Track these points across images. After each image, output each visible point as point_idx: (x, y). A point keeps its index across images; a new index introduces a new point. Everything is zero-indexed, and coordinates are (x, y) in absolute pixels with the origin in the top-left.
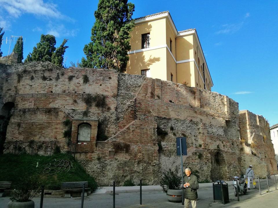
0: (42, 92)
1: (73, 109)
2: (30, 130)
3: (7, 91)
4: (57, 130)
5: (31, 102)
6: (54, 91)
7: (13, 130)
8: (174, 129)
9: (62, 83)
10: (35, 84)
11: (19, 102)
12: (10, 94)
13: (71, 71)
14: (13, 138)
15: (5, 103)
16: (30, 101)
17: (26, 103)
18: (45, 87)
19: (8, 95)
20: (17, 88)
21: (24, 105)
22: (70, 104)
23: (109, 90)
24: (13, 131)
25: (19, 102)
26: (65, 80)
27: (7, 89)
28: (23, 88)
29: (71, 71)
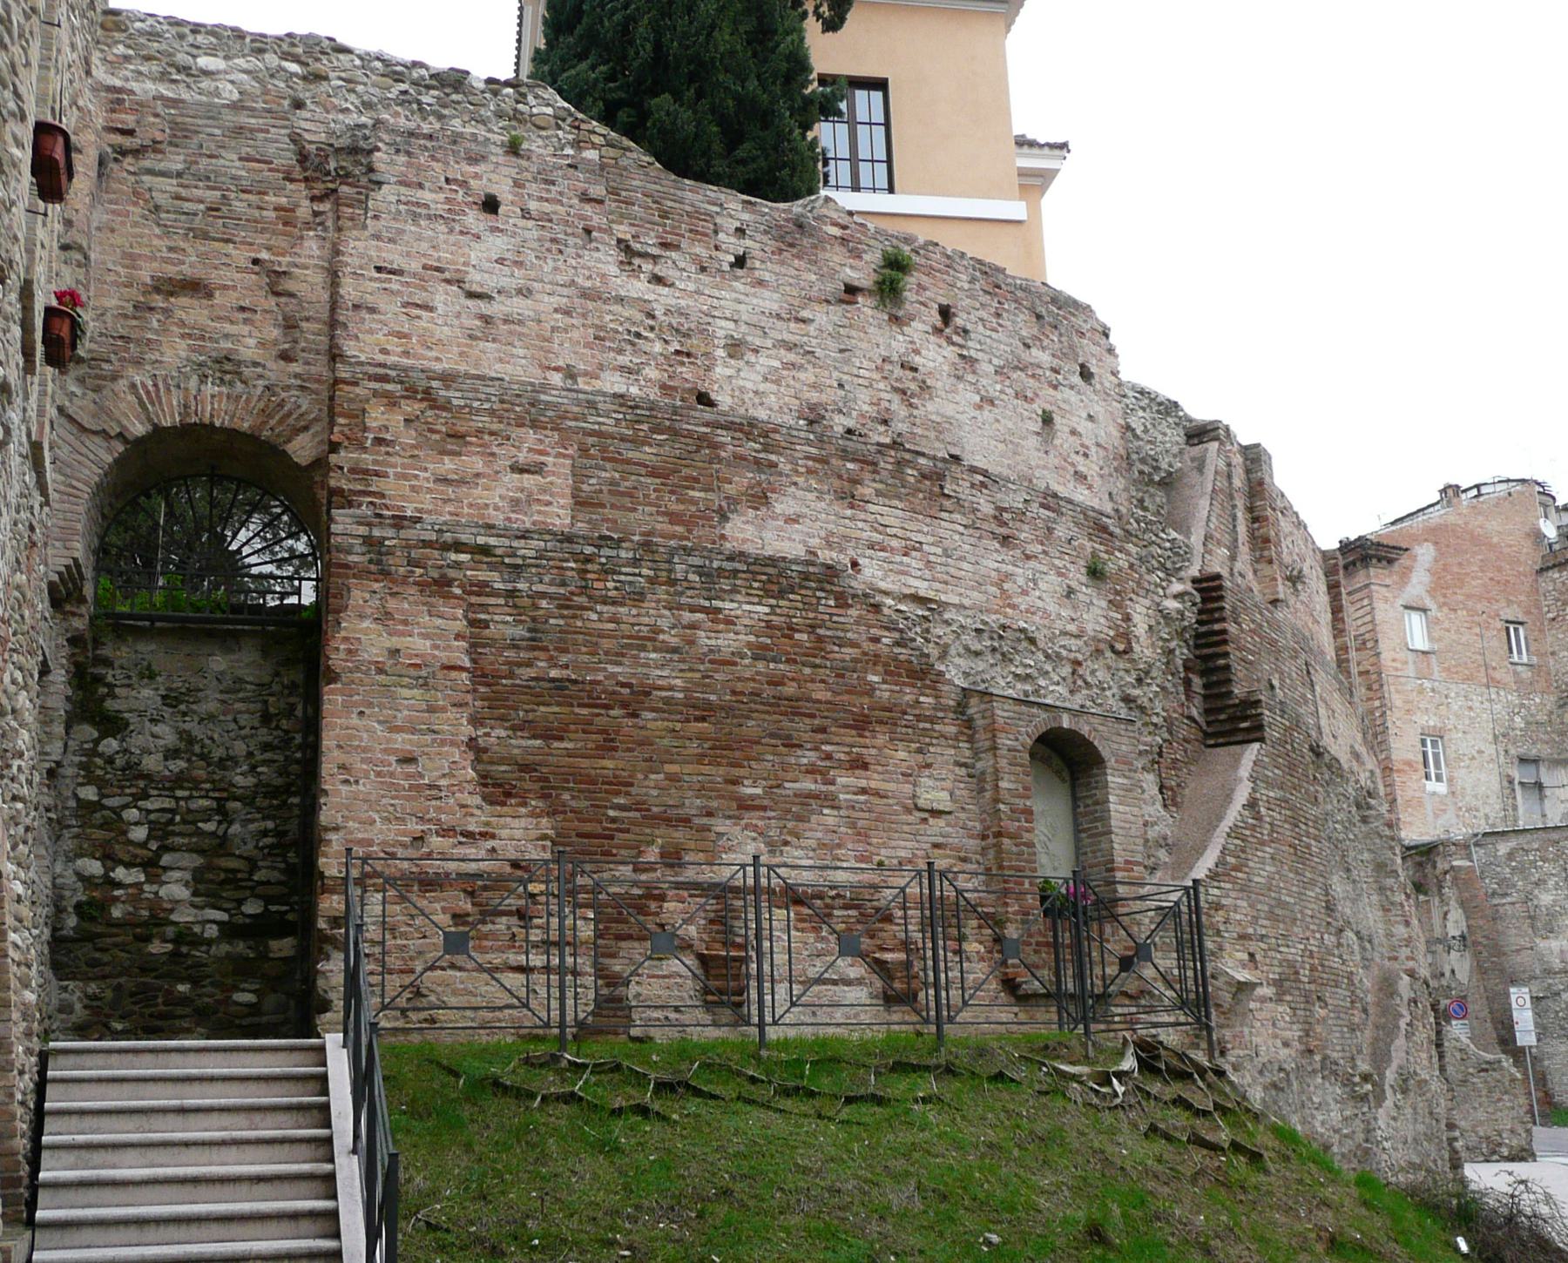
0: (613, 383)
1: (922, 593)
2: (609, 764)
3: (158, 301)
4: (863, 783)
5: (536, 469)
6: (724, 400)
7: (401, 741)
8: (292, 1003)
9: (787, 336)
10: (524, 292)
11: (379, 441)
12: (198, 335)
13: (844, 241)
14: (419, 839)
15: (139, 429)
16: (523, 457)
17: (478, 464)
18: (638, 335)
19: (175, 352)
20: (289, 285)
21: (462, 482)
22: (895, 543)
23: (1090, 468)
24: (409, 760)
25: (379, 441)
26: (805, 314)
27: (145, 275)
28: (391, 308)
29: (844, 241)
